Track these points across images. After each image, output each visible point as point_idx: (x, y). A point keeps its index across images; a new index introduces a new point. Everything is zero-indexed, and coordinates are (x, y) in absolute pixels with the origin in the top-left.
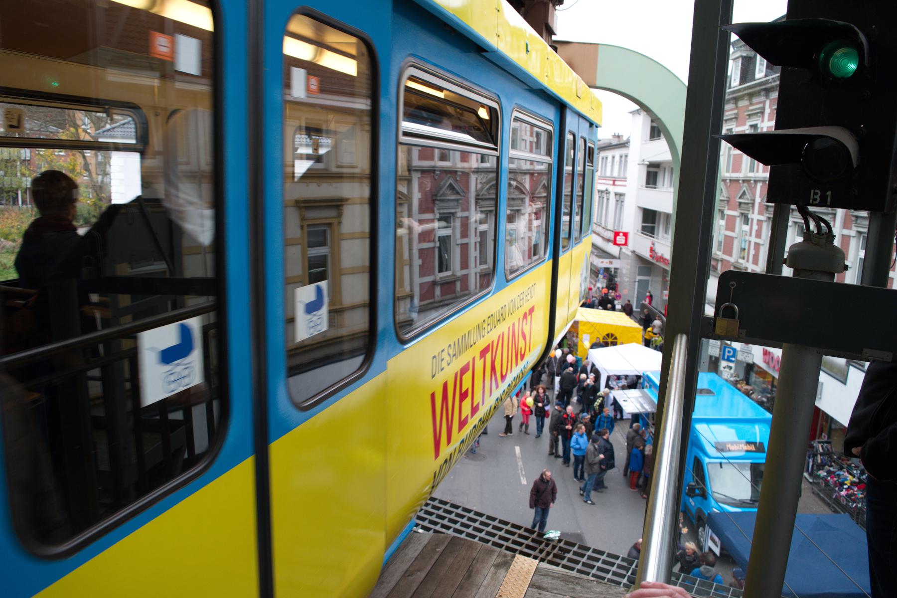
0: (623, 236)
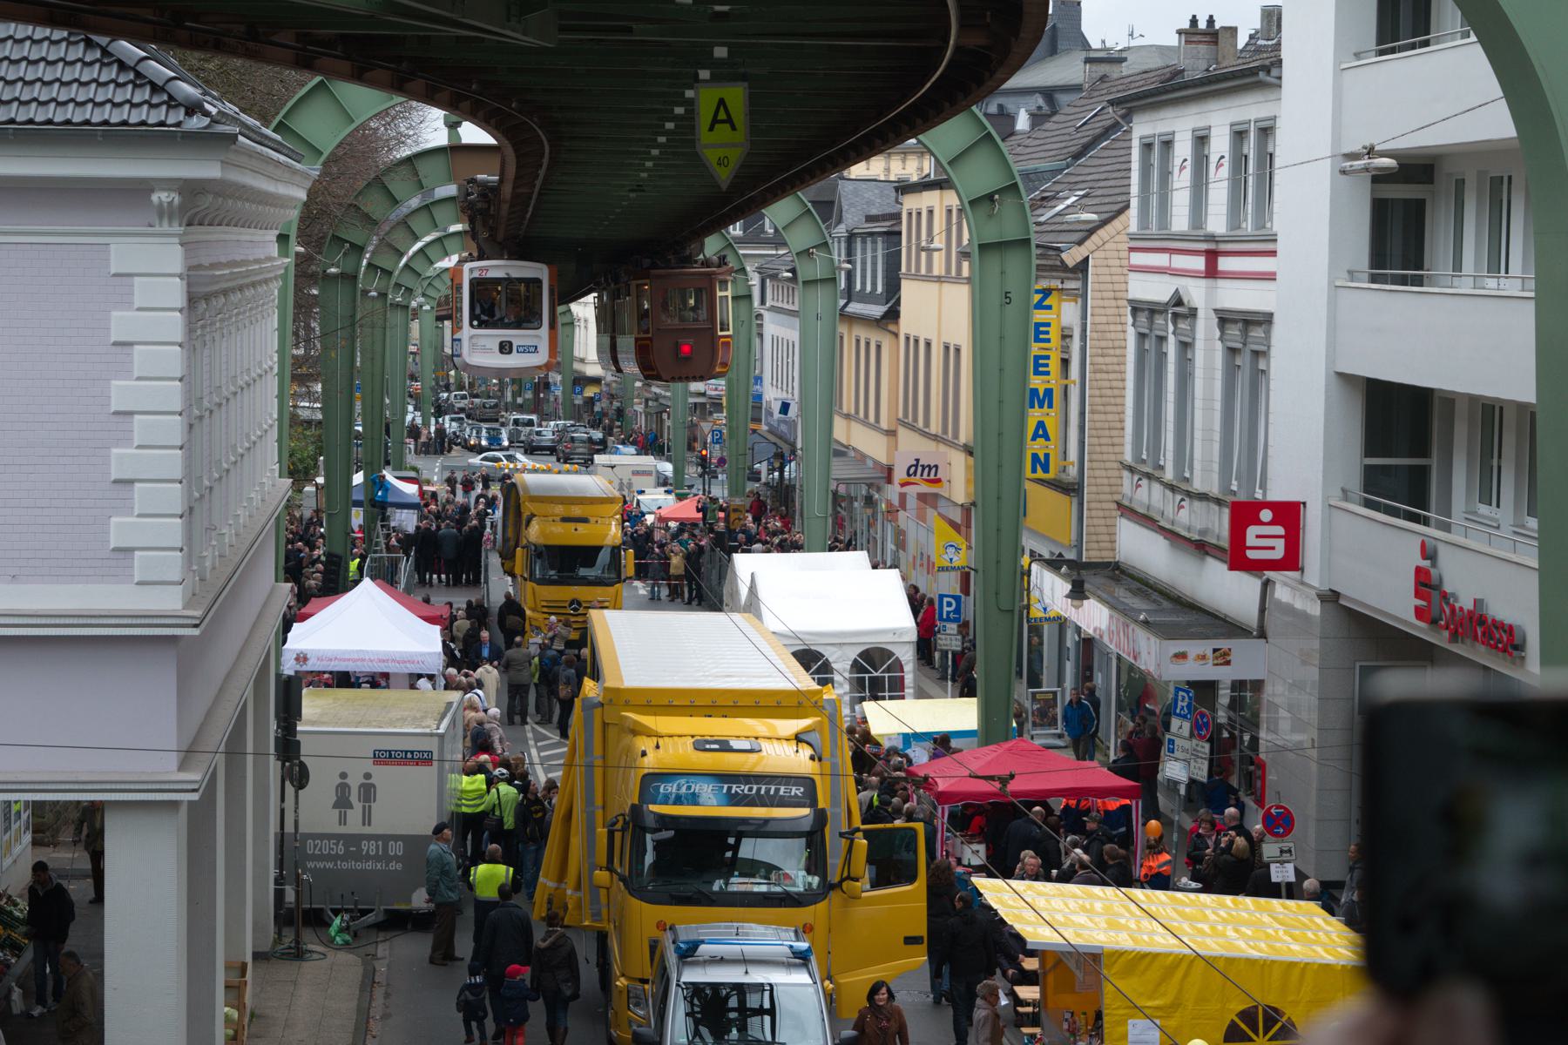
0: (1271, 523)
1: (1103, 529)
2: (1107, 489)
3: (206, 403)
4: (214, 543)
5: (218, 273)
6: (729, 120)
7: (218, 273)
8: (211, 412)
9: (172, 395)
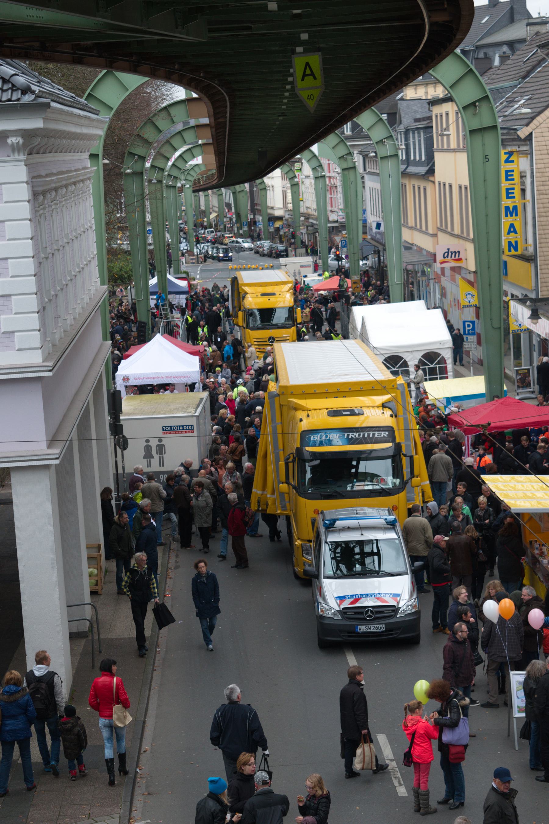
3: (49, 250)
4: (60, 325)
5: (47, 179)
6: (312, 74)
7: (47, 179)
8: (53, 254)
9: (27, 247)
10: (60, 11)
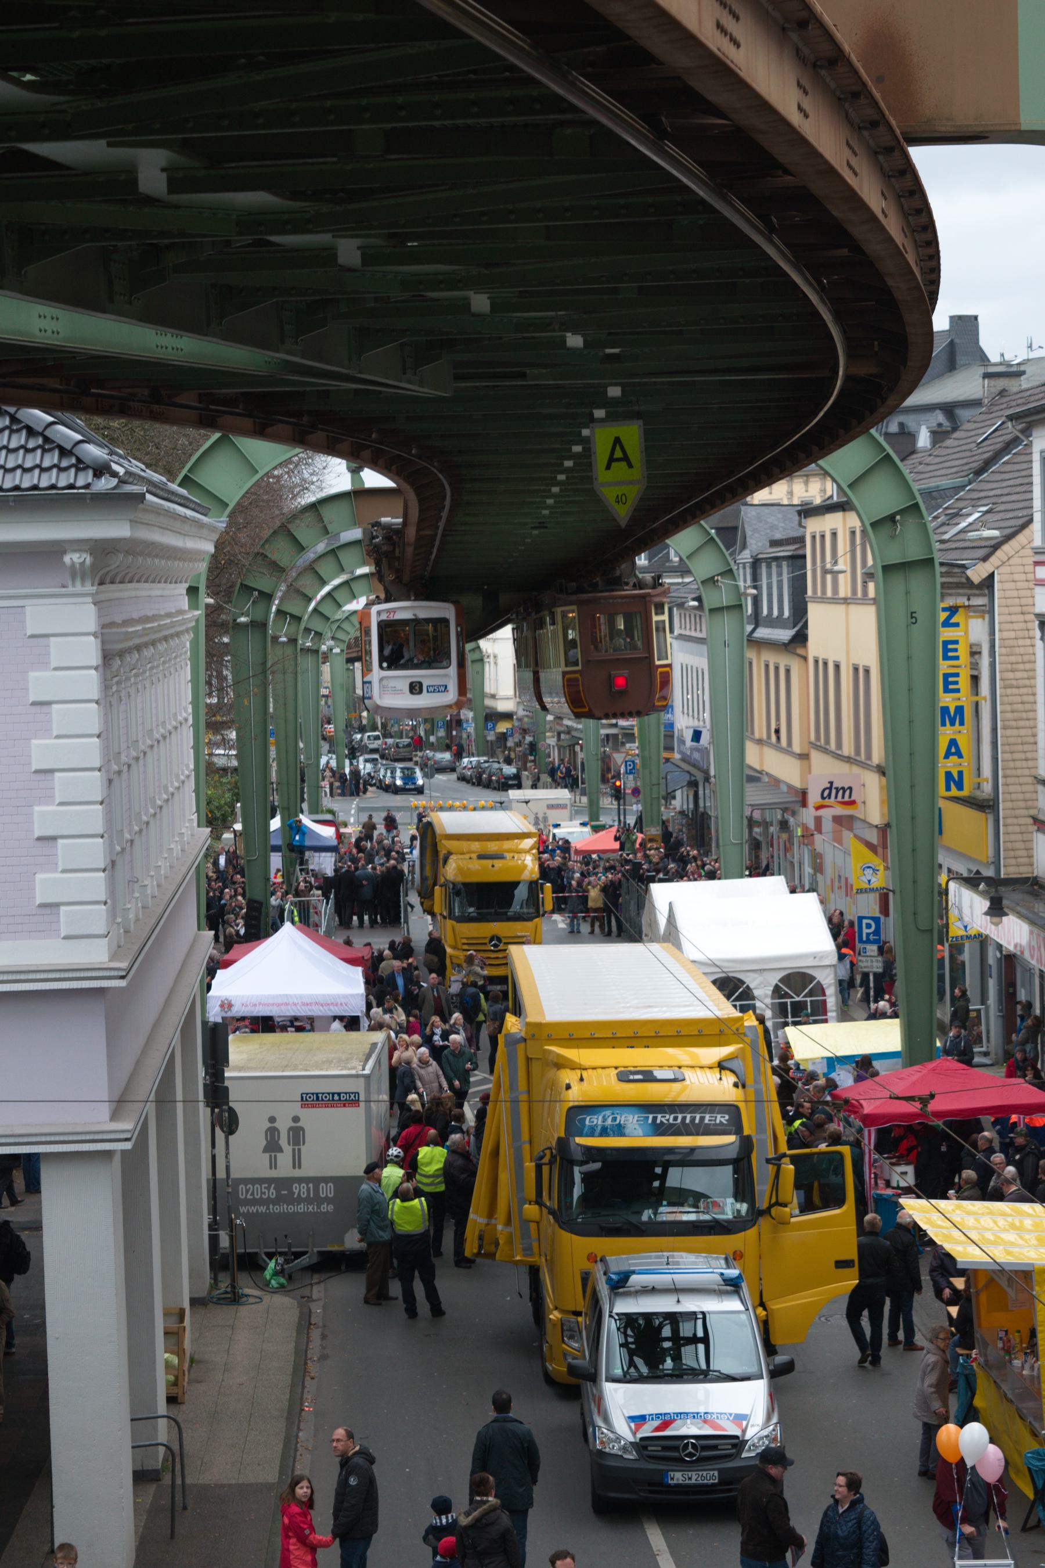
1: (1021, 845)
2: (1022, 804)
3: (124, 758)
4: (137, 895)
5: (130, 630)
6: (626, 458)
7: (130, 630)
8: (129, 766)
9: (91, 751)
10: (223, 342)
